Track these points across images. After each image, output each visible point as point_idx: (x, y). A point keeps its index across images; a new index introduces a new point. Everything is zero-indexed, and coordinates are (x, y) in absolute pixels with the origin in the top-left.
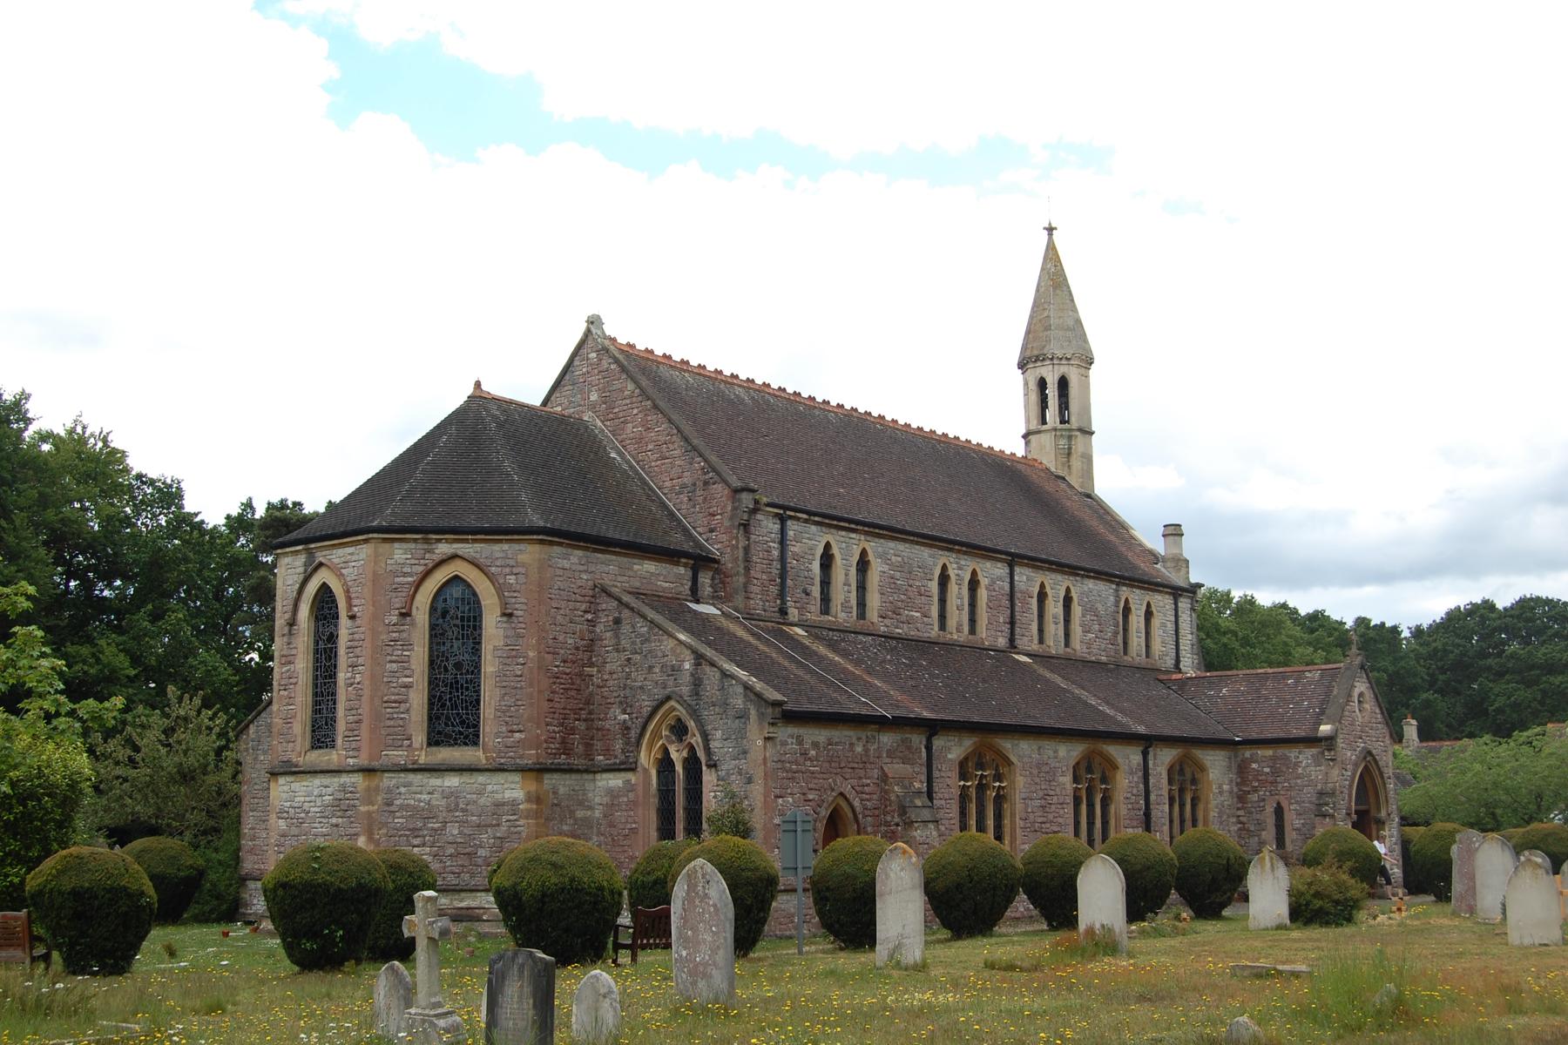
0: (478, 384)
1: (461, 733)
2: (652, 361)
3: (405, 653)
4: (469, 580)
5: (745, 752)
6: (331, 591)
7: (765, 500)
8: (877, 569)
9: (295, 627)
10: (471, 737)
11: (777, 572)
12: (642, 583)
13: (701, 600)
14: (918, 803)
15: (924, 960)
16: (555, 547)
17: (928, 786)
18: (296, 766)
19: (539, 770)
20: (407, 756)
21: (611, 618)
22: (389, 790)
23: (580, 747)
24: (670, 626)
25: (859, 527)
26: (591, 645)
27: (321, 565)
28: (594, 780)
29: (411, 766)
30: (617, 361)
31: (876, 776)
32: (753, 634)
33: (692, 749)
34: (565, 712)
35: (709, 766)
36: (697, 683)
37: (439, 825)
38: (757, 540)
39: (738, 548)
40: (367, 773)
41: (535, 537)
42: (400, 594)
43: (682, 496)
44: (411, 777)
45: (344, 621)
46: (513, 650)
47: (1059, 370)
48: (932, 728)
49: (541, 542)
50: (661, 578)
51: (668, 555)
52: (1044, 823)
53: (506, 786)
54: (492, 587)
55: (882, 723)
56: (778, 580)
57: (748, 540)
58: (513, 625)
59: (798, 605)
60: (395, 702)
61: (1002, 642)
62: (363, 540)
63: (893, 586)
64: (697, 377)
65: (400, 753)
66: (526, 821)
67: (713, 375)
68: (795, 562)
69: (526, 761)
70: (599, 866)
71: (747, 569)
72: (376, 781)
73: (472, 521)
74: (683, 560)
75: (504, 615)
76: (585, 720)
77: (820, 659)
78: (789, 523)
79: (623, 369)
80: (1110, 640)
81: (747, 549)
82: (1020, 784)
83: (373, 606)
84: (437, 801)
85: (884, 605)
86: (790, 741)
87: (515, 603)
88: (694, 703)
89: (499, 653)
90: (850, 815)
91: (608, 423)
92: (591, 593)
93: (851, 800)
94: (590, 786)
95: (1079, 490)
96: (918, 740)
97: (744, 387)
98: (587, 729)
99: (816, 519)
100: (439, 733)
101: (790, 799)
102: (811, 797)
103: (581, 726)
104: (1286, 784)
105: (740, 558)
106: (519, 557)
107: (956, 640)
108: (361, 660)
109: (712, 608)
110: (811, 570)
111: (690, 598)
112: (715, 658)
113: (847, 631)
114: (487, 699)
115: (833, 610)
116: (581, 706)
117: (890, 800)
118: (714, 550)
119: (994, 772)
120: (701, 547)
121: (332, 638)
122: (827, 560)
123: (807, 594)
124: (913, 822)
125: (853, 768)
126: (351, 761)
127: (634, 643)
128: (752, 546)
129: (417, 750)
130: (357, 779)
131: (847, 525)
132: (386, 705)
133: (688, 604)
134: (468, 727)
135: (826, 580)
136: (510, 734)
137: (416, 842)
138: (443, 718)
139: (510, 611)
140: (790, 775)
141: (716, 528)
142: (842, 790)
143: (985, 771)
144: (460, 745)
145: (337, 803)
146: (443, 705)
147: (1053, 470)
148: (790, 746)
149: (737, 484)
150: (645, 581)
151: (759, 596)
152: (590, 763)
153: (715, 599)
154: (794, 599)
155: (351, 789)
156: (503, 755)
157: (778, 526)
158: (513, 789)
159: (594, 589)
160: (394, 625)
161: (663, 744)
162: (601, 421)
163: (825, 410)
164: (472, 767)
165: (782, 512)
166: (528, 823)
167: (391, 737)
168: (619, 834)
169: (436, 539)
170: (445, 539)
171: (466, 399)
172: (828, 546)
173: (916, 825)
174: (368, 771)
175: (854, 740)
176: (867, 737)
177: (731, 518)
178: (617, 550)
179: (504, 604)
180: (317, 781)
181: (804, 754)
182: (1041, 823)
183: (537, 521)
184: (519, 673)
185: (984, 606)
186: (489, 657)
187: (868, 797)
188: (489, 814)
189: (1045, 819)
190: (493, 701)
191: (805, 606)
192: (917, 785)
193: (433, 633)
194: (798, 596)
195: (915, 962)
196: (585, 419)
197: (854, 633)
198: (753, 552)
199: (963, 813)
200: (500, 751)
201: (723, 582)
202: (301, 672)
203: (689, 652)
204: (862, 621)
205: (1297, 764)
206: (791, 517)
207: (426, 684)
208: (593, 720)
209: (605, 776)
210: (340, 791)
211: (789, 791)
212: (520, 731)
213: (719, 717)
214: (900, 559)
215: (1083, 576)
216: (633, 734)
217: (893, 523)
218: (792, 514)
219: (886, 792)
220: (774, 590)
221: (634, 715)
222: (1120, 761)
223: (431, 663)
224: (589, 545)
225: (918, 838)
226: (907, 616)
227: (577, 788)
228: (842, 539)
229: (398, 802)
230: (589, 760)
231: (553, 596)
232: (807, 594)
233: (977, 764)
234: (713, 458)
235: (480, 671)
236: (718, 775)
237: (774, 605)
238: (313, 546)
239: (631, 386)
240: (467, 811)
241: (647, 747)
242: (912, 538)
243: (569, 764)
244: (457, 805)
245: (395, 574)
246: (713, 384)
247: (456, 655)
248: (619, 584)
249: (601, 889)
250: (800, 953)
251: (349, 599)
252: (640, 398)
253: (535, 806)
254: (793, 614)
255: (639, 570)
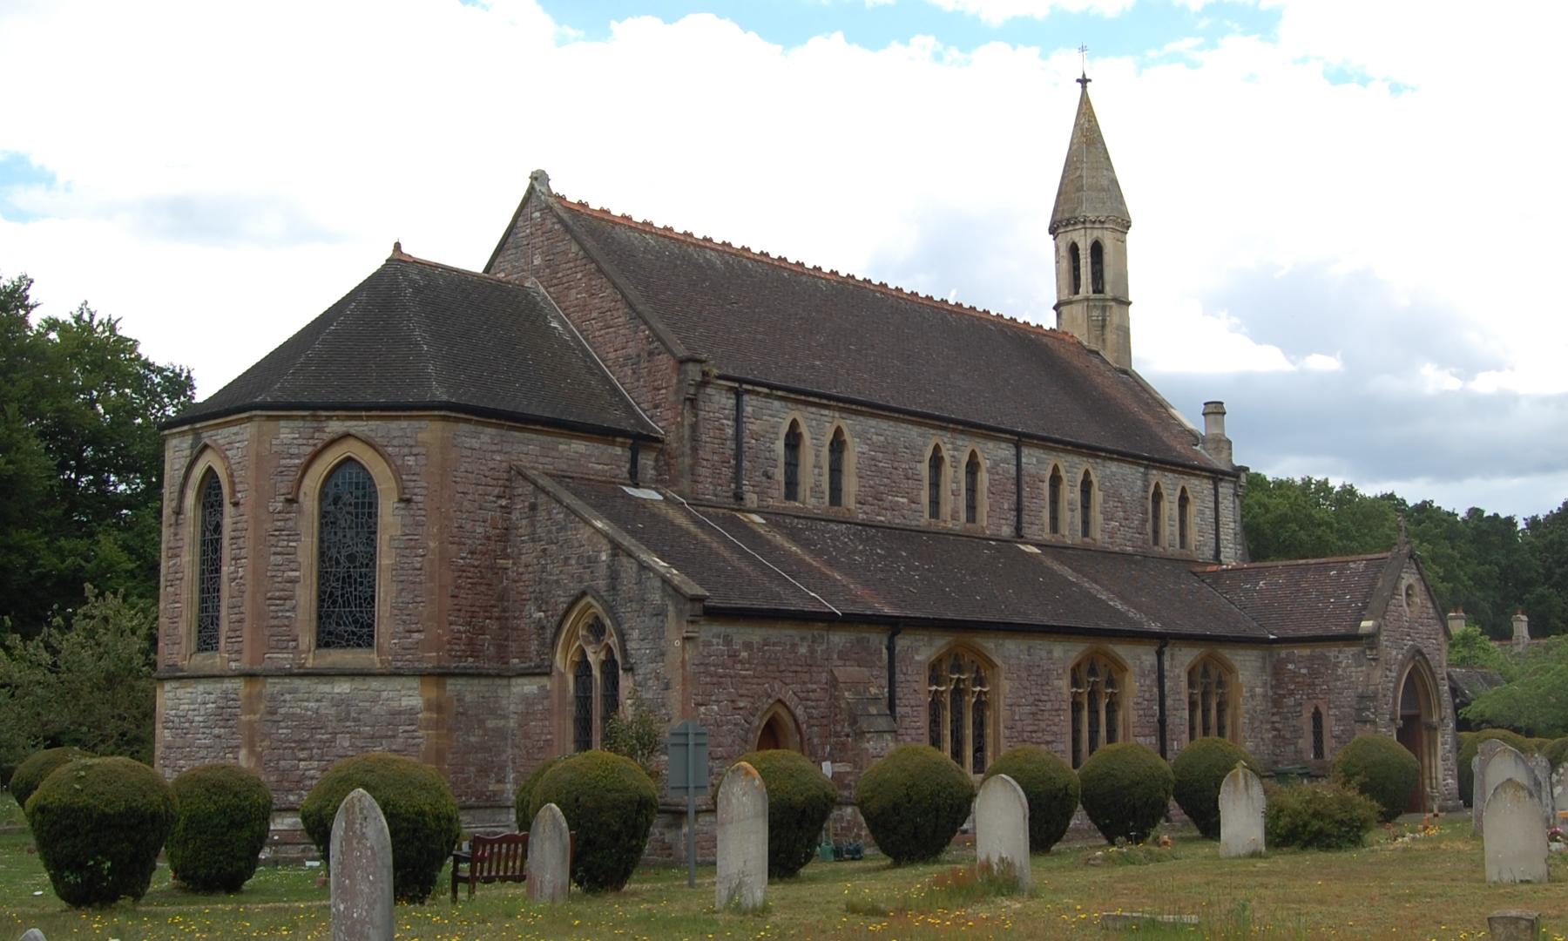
0: (397, 246)
1: (354, 633)
2: (608, 221)
3: (291, 544)
4: (363, 462)
5: (663, 654)
6: (217, 477)
7: (715, 372)
8: (854, 451)
9: (182, 516)
10: (363, 635)
11: (732, 453)
12: (569, 465)
13: (641, 484)
14: (873, 710)
15: (765, 902)
16: (461, 425)
17: (889, 692)
18: (182, 670)
19: (440, 675)
20: (293, 659)
21: (526, 504)
22: (273, 698)
23: (491, 648)
24: (587, 512)
25: (832, 403)
26: (505, 535)
27: (206, 447)
28: (509, 685)
29: (296, 671)
30: (561, 221)
31: (824, 681)
32: (701, 524)
33: (609, 650)
34: (473, 609)
35: (625, 670)
36: (614, 576)
37: (329, 736)
38: (707, 417)
39: (683, 425)
40: (248, 678)
41: (436, 413)
42: (286, 478)
43: (626, 368)
44: (297, 682)
45: (228, 509)
46: (411, 540)
47: (1092, 234)
48: (894, 626)
49: (444, 418)
50: (593, 460)
51: (603, 434)
52: (1035, 732)
53: (403, 692)
54: (388, 470)
55: (830, 620)
56: (733, 462)
57: (696, 416)
58: (412, 512)
59: (757, 489)
60: (280, 598)
61: (1007, 531)
62: (247, 418)
63: (873, 468)
64: (661, 239)
65: (286, 655)
66: (424, 732)
67: (682, 238)
68: (753, 441)
69: (425, 665)
70: (423, 787)
71: (695, 450)
72: (259, 686)
73: (370, 398)
74: (619, 440)
75: (401, 500)
76: (497, 619)
77: (770, 549)
78: (746, 398)
79: (567, 229)
80: (1137, 528)
81: (694, 427)
82: (1005, 689)
83: (256, 491)
84: (327, 709)
85: (863, 489)
86: (715, 641)
87: (414, 488)
88: (611, 598)
89: (396, 544)
90: (791, 724)
91: (552, 290)
92: (505, 476)
93: (792, 708)
94: (502, 693)
95: (1115, 365)
96: (877, 640)
97: (717, 251)
98: (500, 629)
99: (780, 393)
100: (330, 633)
101: (716, 708)
102: (741, 705)
103: (493, 625)
104: (1325, 687)
105: (686, 437)
106: (419, 435)
107: (951, 529)
108: (243, 553)
109: (653, 492)
110: (774, 451)
111: (629, 482)
112: (633, 548)
113: (816, 519)
114: (382, 595)
115: (801, 496)
116: (493, 602)
117: (840, 708)
118: (658, 428)
119: (973, 676)
120: (645, 425)
121: (218, 528)
122: (793, 440)
123: (769, 478)
124: (864, 732)
125: (796, 672)
126: (233, 665)
127: (550, 532)
128: (701, 424)
129: (303, 652)
130: (238, 685)
131: (817, 400)
132: (268, 602)
133: (624, 488)
134: (362, 626)
135: (793, 462)
136: (407, 634)
137: (302, 755)
138: (334, 616)
139: (408, 496)
140: (715, 680)
141: (660, 404)
142: (781, 697)
143: (963, 674)
144: (353, 647)
145: (219, 711)
146: (334, 602)
147: (1085, 343)
148: (715, 647)
149: (682, 352)
150: (572, 463)
151: (709, 480)
152: (504, 666)
153: (658, 483)
154: (752, 483)
155: (233, 696)
156: (399, 657)
157: (732, 402)
158: (410, 696)
159: (509, 472)
160: (279, 513)
161: (580, 646)
162: (544, 287)
163: (815, 276)
164: (366, 671)
165: (737, 385)
166: (428, 735)
167: (276, 638)
168: (533, 747)
169: (326, 416)
170: (337, 416)
171: (384, 262)
172: (794, 424)
173: (868, 736)
174: (250, 676)
175: (797, 640)
176: (813, 636)
177: (677, 392)
178: (538, 427)
179: (402, 489)
180: (201, 687)
181: (734, 656)
182: (1031, 732)
183: (442, 395)
184: (418, 566)
185: (985, 490)
186: (385, 548)
187: (813, 704)
188: (385, 724)
189: (1035, 728)
190: (389, 599)
191: (766, 490)
192: (873, 690)
193: (324, 521)
194: (757, 479)
195: (755, 905)
196: (526, 285)
197: (824, 520)
198: (702, 430)
199: (935, 722)
200: (397, 654)
201: (667, 464)
202: (187, 566)
203: (605, 541)
204: (836, 508)
205: (1336, 665)
206: (747, 392)
207: (315, 579)
208: (507, 619)
209: (520, 681)
210: (222, 698)
211: (713, 698)
212: (418, 631)
213: (636, 614)
214: (882, 439)
215: (1104, 458)
216: (549, 634)
217: (877, 400)
218: (750, 387)
219: (837, 699)
220: (727, 472)
221: (550, 613)
222: (1129, 662)
223: (322, 555)
224: (503, 422)
225: (871, 751)
226: (891, 502)
227: (487, 695)
228: (812, 416)
229: (282, 711)
230: (503, 663)
231: (458, 479)
232: (769, 478)
233: (953, 666)
234: (660, 326)
235: (375, 563)
236: (635, 680)
237: (728, 489)
238: (198, 425)
239: (575, 248)
240: (359, 720)
241: (563, 648)
242: (896, 415)
243: (477, 668)
244: (348, 713)
245: (280, 455)
246: (680, 247)
247: (349, 546)
248: (540, 466)
249: (422, 814)
250: (691, 885)
251: (232, 484)
252: (584, 261)
253: (435, 716)
254: (751, 499)
255: (566, 450)
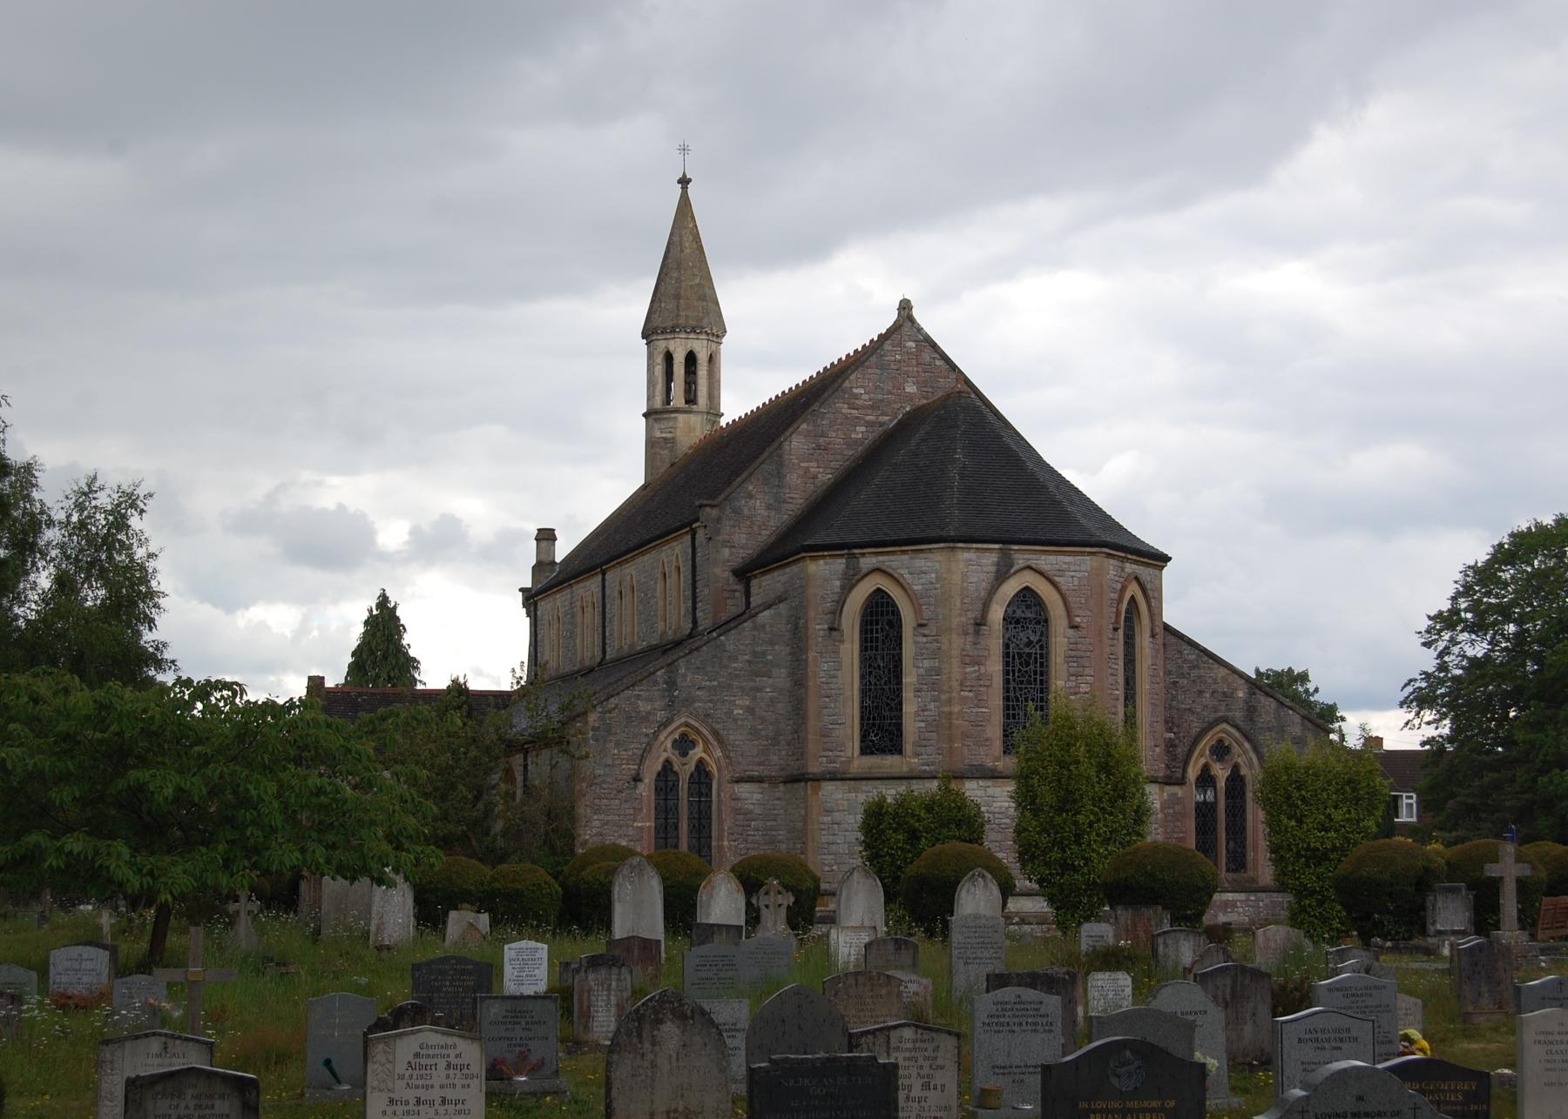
88: (1249, 727)
203: (1243, 681)
